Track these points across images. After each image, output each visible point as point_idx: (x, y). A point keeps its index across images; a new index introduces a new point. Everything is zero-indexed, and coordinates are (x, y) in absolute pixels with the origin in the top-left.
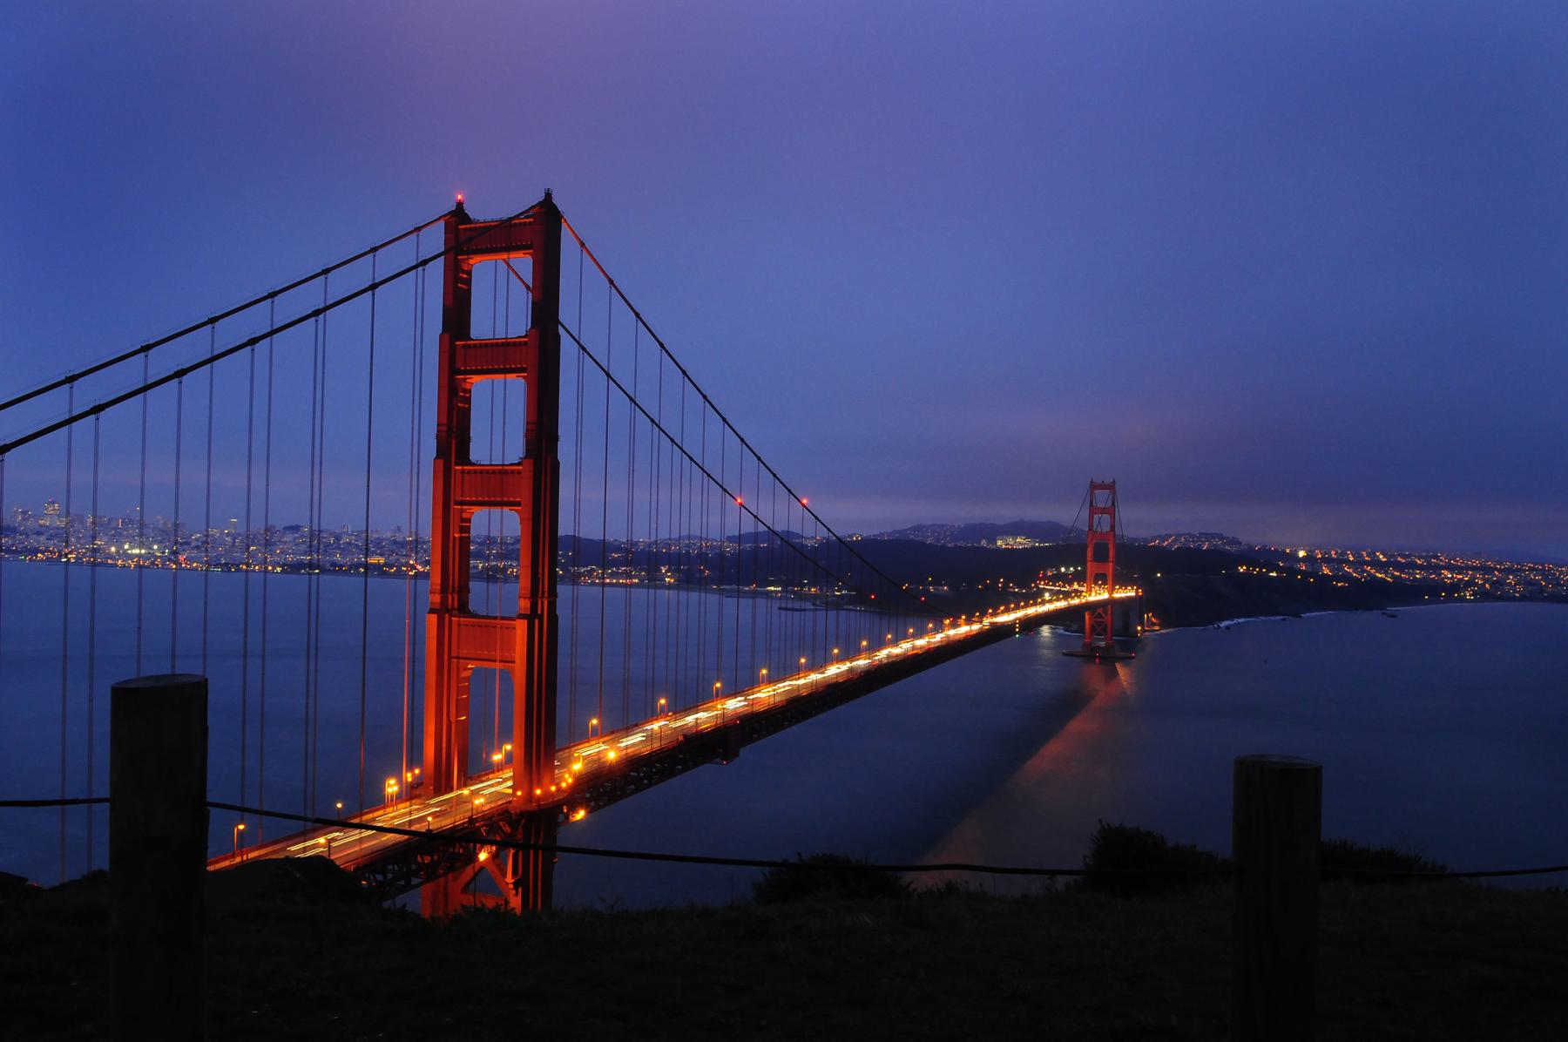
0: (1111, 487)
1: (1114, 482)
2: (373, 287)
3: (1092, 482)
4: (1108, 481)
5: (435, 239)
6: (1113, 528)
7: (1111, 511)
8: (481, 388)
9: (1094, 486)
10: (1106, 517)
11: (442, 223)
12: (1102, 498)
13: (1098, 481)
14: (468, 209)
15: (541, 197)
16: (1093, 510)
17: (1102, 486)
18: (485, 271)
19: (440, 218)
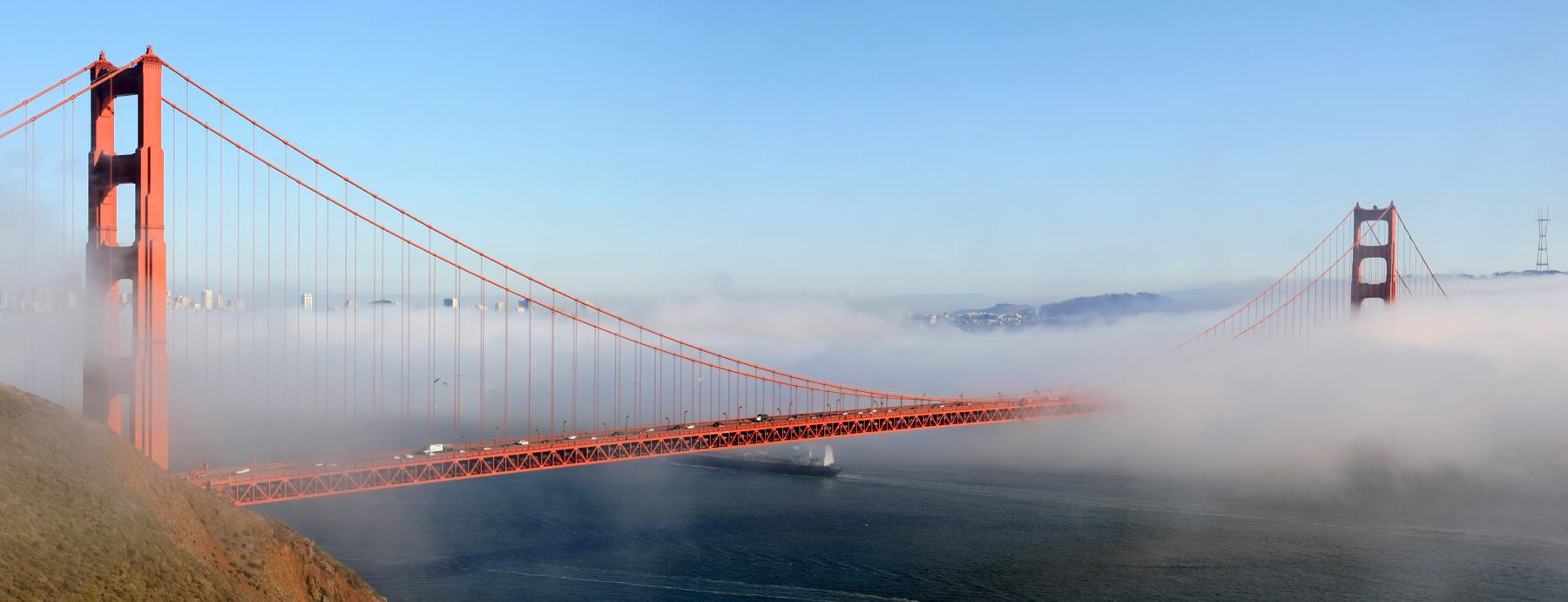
0: (1388, 215)
1: (1392, 208)
4: (1379, 208)
5: (85, 81)
6: (1390, 275)
7: (1386, 252)
9: (1361, 215)
10: (1382, 262)
11: (89, 71)
12: (1375, 233)
13: (1370, 208)
14: (108, 59)
15: (143, 53)
16: (1361, 253)
17: (1374, 214)
19: (86, 69)
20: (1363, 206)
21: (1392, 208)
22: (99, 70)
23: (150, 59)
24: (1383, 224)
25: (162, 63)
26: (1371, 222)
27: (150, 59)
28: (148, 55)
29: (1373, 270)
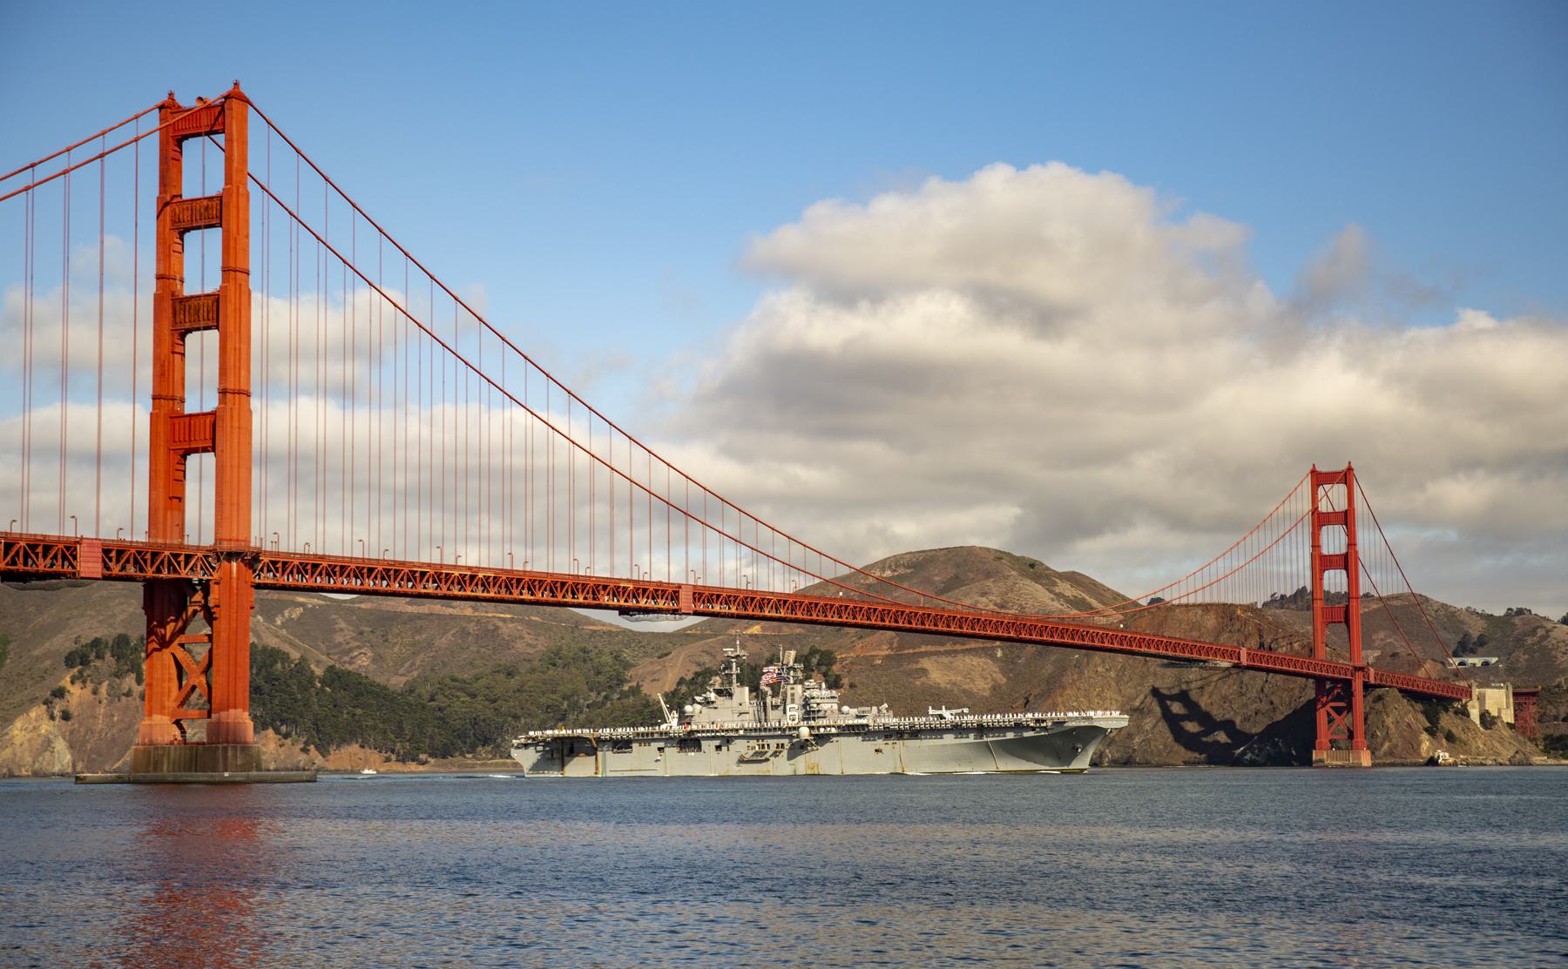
0: (1346, 477)
1: (1350, 469)
2: (102, 156)
3: (1313, 472)
7: (1346, 518)
8: (192, 238)
11: (158, 110)
12: (1333, 497)
16: (1320, 520)
18: (191, 147)
20: (1318, 469)
21: (1350, 469)
22: (168, 108)
23: (236, 96)
24: (1342, 488)
25: (248, 102)
26: (1327, 487)
27: (236, 96)
28: (236, 90)
29: (1333, 541)
